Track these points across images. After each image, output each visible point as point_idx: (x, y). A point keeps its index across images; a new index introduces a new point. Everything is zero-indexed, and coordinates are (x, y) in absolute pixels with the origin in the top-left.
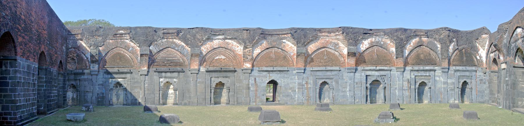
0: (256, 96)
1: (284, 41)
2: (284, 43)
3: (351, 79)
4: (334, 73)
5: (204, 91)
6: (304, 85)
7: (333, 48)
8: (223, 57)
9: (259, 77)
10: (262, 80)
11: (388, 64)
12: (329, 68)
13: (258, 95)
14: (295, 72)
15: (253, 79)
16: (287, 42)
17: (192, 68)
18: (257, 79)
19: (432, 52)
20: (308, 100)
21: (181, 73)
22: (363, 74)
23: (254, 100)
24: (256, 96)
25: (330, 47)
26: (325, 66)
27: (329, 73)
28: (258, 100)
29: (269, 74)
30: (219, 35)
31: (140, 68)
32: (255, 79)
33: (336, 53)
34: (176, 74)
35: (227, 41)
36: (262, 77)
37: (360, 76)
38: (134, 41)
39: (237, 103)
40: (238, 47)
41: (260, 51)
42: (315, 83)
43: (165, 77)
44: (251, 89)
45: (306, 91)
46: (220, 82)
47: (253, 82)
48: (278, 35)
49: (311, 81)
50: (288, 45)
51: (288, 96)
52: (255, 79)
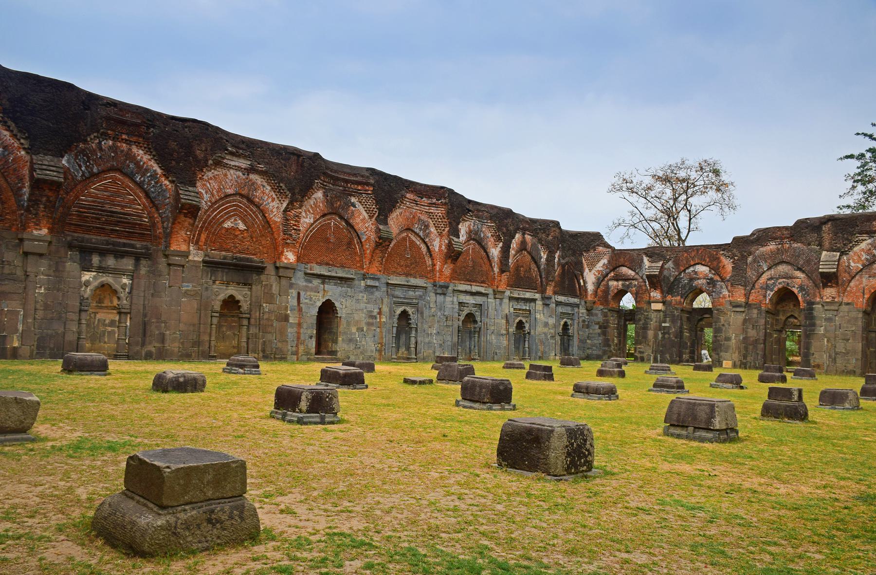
0: (298, 338)
1: (353, 200)
2: (354, 205)
3: (440, 309)
4: (419, 293)
5: (196, 321)
6: (376, 318)
7: (421, 234)
8: (242, 226)
9: (306, 289)
10: (311, 299)
11: (483, 282)
12: (413, 281)
13: (302, 338)
14: (363, 283)
15: (295, 294)
16: (360, 207)
17: (174, 247)
18: (302, 293)
19: (533, 266)
20: (380, 351)
21: (143, 262)
22: (455, 299)
23: (294, 349)
24: (298, 338)
25: (417, 231)
26: (407, 275)
27: (411, 293)
28: (301, 348)
29: (323, 283)
30: (238, 156)
31: (24, 227)
32: (299, 294)
33: (423, 246)
34: (128, 264)
35: (253, 177)
36: (312, 290)
37: (450, 302)
38: (10, 123)
39: (264, 357)
40: (273, 200)
41: (312, 221)
42: (392, 312)
43: (101, 269)
44: (291, 320)
45: (378, 330)
46: (232, 297)
47: (295, 303)
48: (347, 181)
49: (385, 309)
50: (360, 214)
51: (351, 340)
52: (299, 294)
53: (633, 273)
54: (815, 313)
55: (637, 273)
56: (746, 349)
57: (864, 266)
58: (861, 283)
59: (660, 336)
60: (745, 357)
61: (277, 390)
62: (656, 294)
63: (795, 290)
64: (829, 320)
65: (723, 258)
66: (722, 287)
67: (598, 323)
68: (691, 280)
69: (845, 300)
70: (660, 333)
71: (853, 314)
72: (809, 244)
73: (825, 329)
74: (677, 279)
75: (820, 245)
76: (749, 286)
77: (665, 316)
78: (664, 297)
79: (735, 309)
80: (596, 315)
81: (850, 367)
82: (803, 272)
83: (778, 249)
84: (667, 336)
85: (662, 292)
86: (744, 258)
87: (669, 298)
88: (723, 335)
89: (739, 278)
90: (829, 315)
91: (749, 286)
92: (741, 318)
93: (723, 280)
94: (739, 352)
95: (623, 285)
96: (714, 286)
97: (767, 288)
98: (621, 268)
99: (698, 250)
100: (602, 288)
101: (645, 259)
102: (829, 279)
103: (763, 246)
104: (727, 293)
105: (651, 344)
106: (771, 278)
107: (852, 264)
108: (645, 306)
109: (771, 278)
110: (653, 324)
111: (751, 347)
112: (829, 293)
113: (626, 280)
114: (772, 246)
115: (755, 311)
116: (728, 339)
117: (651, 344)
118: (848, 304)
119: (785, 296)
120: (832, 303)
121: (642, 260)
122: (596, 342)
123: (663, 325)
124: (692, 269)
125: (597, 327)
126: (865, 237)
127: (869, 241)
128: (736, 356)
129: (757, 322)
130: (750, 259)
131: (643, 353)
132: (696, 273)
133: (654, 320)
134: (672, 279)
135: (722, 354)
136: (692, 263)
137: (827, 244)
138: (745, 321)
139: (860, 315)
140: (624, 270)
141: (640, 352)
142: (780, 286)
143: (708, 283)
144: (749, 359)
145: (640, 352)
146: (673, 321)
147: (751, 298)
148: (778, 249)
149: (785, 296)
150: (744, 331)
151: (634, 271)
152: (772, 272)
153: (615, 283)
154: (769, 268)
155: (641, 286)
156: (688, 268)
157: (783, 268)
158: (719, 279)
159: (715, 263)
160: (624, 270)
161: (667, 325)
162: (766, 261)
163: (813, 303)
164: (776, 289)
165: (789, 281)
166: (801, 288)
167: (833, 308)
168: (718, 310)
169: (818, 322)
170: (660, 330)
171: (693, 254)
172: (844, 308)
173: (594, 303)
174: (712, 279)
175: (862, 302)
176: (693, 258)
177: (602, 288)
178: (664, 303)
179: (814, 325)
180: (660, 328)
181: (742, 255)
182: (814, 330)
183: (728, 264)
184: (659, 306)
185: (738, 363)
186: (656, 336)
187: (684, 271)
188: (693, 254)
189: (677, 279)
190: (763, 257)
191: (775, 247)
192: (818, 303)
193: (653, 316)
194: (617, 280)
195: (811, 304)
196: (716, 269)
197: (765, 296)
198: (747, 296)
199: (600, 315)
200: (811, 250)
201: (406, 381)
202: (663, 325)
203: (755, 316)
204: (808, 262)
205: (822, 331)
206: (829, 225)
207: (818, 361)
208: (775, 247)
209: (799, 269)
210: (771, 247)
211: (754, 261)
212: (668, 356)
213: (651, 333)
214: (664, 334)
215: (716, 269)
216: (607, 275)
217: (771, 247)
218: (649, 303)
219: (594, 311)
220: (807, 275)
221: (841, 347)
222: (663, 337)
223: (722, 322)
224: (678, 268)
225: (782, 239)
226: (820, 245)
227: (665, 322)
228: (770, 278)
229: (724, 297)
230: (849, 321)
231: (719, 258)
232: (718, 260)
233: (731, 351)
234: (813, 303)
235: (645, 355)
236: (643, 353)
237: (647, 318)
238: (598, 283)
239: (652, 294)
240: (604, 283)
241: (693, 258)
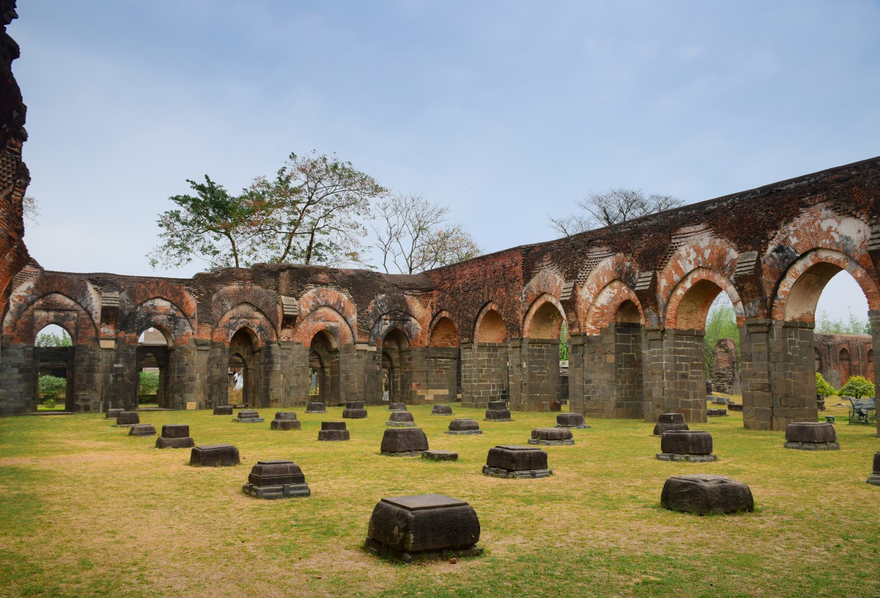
53: (71, 303)
54: (273, 352)
55: (80, 304)
56: (211, 388)
57: (311, 311)
58: (308, 326)
59: (111, 379)
60: (210, 397)
61: (378, 507)
62: (108, 330)
63: (255, 330)
64: (284, 357)
65: (187, 294)
66: (185, 325)
67: (18, 366)
68: (149, 315)
69: (296, 340)
70: (111, 375)
71: (303, 352)
72: (267, 288)
73: (281, 367)
74: (133, 314)
75: (277, 289)
76: (214, 323)
77: (118, 356)
78: (117, 333)
79: (200, 348)
80: (15, 355)
81: (301, 399)
82: (262, 313)
83: (241, 290)
84: (119, 379)
85: (115, 328)
86: (209, 296)
87: (122, 334)
88: (187, 375)
89: (206, 315)
90: (285, 353)
91: (214, 323)
92: (205, 357)
93: (186, 316)
94: (204, 392)
95: (55, 316)
96: (176, 323)
97: (229, 327)
98: (54, 295)
99: (158, 283)
100: (24, 319)
101: (90, 287)
102: (290, 321)
103: (226, 285)
104: (191, 331)
105: (99, 389)
106: (233, 318)
107: (302, 309)
108: (90, 344)
109: (233, 318)
110: (102, 365)
111: (216, 386)
112: (286, 334)
113: (60, 310)
114: (234, 287)
115: (219, 350)
116: (192, 379)
117: (99, 389)
118: (298, 343)
119: (244, 335)
120: (288, 342)
121: (86, 288)
122: (13, 390)
123: (115, 366)
124: (150, 303)
125: (16, 370)
126: (312, 286)
127: (314, 290)
128: (201, 397)
129: (221, 361)
130: (214, 297)
131: (88, 400)
132: (155, 307)
133: (104, 360)
134: (126, 313)
135: (187, 395)
136: (151, 296)
137: (283, 289)
138: (210, 360)
139: (308, 353)
140: (59, 298)
141: (83, 400)
142: (241, 326)
143: (170, 320)
144: (214, 398)
145: (83, 400)
146: (127, 362)
147: (214, 337)
148: (241, 290)
149: (244, 335)
150: (209, 370)
151: (75, 300)
152: (235, 311)
153: (44, 314)
154: (232, 308)
155: (83, 319)
156: (145, 301)
157: (244, 309)
158: (181, 315)
159: (178, 299)
160: (59, 298)
161: (120, 366)
162: (230, 301)
163: (271, 343)
164: (237, 328)
165: (250, 321)
166: (261, 328)
167: (288, 347)
168: (181, 348)
169: (275, 360)
170: (111, 372)
171: (152, 286)
172: (296, 347)
173: (12, 338)
174: (173, 315)
175: (308, 341)
176: (152, 291)
177: (24, 319)
178: (116, 340)
179: (271, 362)
180: (112, 370)
181: (208, 293)
182: (272, 368)
183: (192, 302)
184: (111, 344)
185: (203, 404)
186: (106, 380)
187: (141, 304)
188: (152, 286)
189: (133, 314)
190: (227, 296)
191: (238, 287)
192: (275, 343)
193: (102, 355)
194: (48, 310)
195: (269, 343)
196: (179, 305)
197: (228, 335)
198: (212, 333)
199: (20, 354)
200: (269, 294)
201: (454, 457)
202: (115, 366)
203: (219, 354)
204: (267, 304)
205: (278, 367)
206: (287, 273)
207: (276, 396)
208: (238, 287)
209: (259, 310)
210: (234, 287)
211: (219, 299)
212: (121, 402)
213: (98, 377)
214: (116, 376)
215: (179, 305)
216: (33, 302)
217: (234, 287)
218: (97, 340)
219: (9, 350)
220: (266, 316)
221: (293, 383)
222: (115, 380)
223: (186, 361)
224: (134, 301)
225: (245, 280)
226: (277, 289)
227: (117, 363)
228: (233, 315)
229: (188, 335)
230: (299, 358)
231: (182, 293)
232: (181, 295)
233: (196, 392)
234: (271, 343)
235: (91, 403)
236: (88, 400)
237: (93, 358)
238: (20, 310)
239: (102, 330)
240: (28, 312)
241: (152, 291)
